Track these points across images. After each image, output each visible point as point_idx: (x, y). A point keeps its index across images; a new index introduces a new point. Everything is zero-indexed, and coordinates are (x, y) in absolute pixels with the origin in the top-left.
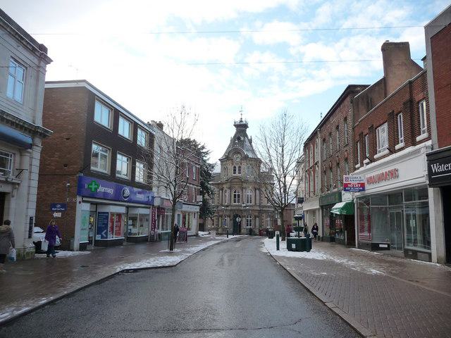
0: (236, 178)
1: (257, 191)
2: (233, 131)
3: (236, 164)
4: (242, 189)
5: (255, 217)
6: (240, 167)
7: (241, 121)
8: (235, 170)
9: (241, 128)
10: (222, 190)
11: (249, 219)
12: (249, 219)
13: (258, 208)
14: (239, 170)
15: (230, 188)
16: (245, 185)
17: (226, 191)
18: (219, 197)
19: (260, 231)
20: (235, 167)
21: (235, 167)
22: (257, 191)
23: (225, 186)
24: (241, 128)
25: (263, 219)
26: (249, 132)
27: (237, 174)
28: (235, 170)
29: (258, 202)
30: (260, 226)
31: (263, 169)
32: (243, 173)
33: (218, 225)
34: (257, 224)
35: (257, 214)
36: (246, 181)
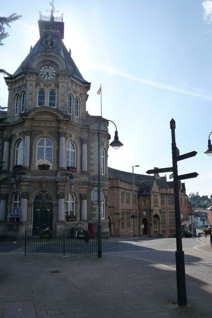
1: (85, 146)
3: (47, 86)
7: (52, 18)
8: (42, 98)
10: (10, 140)
13: (85, 178)
14: (52, 98)
16: (64, 127)
17: (19, 141)
20: (42, 92)
21: (42, 92)
23: (17, 132)
28: (42, 98)
30: (90, 216)
34: (85, 217)
35: (84, 191)
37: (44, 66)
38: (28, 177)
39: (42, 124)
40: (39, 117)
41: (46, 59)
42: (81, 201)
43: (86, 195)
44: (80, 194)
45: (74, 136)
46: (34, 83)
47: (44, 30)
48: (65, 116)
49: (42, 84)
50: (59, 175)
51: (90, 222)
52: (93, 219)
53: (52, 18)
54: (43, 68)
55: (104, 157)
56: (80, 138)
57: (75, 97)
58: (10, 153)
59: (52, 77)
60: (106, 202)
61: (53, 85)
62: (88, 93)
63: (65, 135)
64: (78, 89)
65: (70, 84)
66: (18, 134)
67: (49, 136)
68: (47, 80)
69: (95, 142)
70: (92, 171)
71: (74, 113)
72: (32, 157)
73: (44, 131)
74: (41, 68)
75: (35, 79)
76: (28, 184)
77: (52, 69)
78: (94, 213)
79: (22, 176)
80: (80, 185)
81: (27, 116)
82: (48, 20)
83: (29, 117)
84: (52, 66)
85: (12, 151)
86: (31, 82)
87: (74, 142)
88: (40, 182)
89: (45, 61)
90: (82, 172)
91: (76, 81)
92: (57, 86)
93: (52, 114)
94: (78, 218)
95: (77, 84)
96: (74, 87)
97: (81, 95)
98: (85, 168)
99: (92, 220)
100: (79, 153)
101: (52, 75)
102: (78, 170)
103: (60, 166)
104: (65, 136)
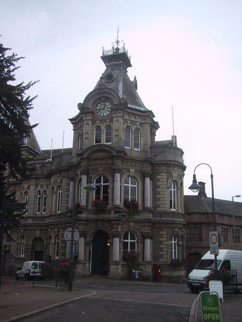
0: (100, 148)
1: (148, 180)
2: (101, 68)
4: (114, 172)
5: (144, 237)
6: (109, 127)
9: (117, 61)
11: (129, 241)
12: (129, 241)
15: (87, 173)
16: (119, 164)
18: (68, 196)
19: (156, 268)
20: (99, 128)
22: (148, 180)
24: (117, 61)
25: (161, 242)
26: (131, 73)
27: (103, 142)
29: (149, 204)
31: (161, 136)
32: (114, 140)
33: (64, 254)
35: (146, 230)
36: (121, 155)
37: (100, 103)
38: (84, 216)
39: (99, 162)
40: (95, 155)
41: (101, 96)
42: (144, 240)
43: (148, 233)
44: (142, 232)
45: (132, 170)
46: (90, 122)
47: (107, 64)
48: (117, 151)
49: (98, 122)
50: (112, 213)
51: (156, 263)
52: (160, 260)
53: (118, 49)
54: (100, 105)
55: (175, 190)
56: (141, 171)
57: (133, 129)
58: (74, 191)
59: (108, 113)
60: (178, 241)
61: (108, 121)
62: (155, 119)
63: (120, 171)
64: (138, 120)
65: (127, 117)
66: (79, 173)
67: (104, 173)
68: (103, 116)
69: (162, 174)
70: (159, 207)
71: (133, 145)
72: (89, 196)
73: (100, 169)
74: (97, 106)
75: (90, 118)
76: (84, 222)
77: (108, 104)
78: (160, 253)
79: (79, 215)
80: (141, 222)
81: (82, 156)
82: (110, 53)
83: (85, 156)
84: (106, 101)
85: (76, 190)
86: (87, 122)
87: (133, 176)
88: (96, 221)
89: (100, 98)
90: (146, 210)
91: (133, 112)
92: (112, 120)
93: (106, 151)
94: (140, 259)
95: (135, 115)
96: (133, 119)
97: (141, 124)
98: (149, 204)
99: (158, 261)
100: (141, 188)
101: (108, 111)
102: (140, 207)
103: (115, 204)
104: (119, 172)
